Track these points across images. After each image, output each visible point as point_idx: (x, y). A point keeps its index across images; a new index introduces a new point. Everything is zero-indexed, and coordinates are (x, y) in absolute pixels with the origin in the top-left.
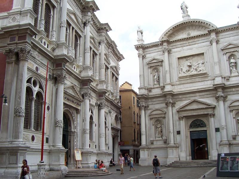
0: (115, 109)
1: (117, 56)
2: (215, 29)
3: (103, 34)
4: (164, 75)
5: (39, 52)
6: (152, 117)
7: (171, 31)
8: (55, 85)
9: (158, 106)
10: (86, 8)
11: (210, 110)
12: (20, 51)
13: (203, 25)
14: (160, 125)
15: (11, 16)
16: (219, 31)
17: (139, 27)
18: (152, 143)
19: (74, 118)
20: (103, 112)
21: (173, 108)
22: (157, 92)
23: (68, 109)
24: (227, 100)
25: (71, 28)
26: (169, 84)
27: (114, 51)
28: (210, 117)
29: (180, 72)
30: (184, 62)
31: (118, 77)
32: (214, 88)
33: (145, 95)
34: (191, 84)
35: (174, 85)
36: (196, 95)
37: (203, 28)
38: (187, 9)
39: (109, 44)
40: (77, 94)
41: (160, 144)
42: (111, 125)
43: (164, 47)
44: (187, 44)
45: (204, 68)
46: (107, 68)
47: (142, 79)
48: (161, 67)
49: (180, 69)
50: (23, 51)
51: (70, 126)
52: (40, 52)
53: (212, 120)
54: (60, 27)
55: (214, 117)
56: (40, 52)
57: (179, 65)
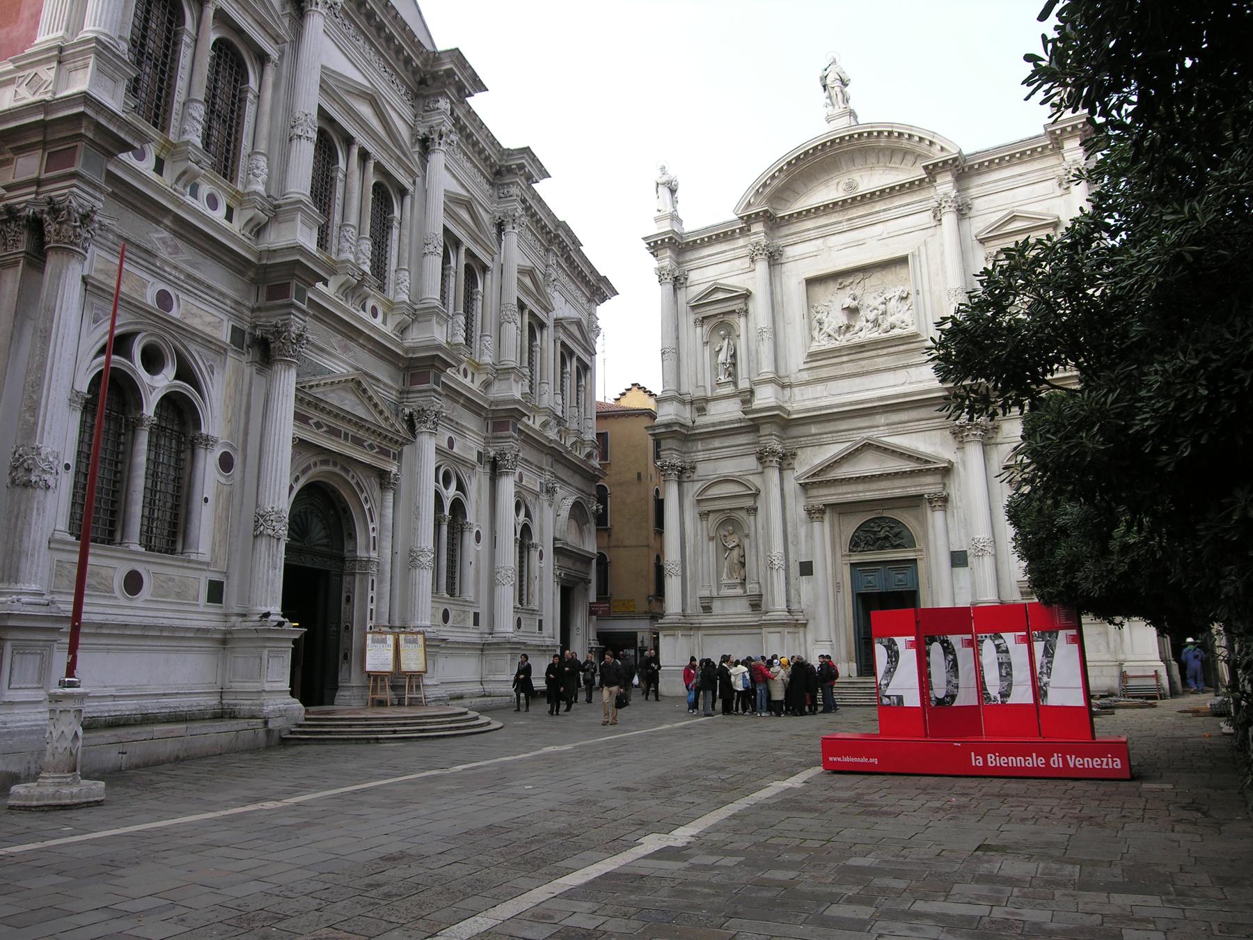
0: (577, 481)
1: (588, 284)
2: (955, 160)
3: (514, 190)
4: (753, 348)
5: (175, 233)
6: (707, 507)
7: (782, 176)
8: (259, 372)
9: (728, 468)
10: (430, 82)
11: (929, 479)
12: (48, 213)
13: (904, 143)
14: (737, 541)
15: (26, 73)
16: (971, 167)
17: (663, 168)
18: (707, 609)
19: (366, 507)
20: (507, 486)
21: (787, 473)
22: (726, 411)
23: (337, 470)
24: (999, 440)
25: (355, 150)
26: (770, 381)
27: (569, 259)
28: (929, 511)
29: (815, 334)
30: (830, 298)
31: (593, 361)
32: (946, 393)
33: (682, 425)
34: (857, 380)
35: (790, 386)
36: (875, 423)
37: (908, 157)
38: (847, 89)
39: (550, 232)
40: (381, 412)
41: (737, 610)
42: (555, 539)
43: (754, 239)
44: (845, 226)
45: (907, 317)
46: (536, 326)
47: (671, 363)
48: (743, 320)
49: (815, 323)
50: (60, 210)
51: (352, 536)
52: (181, 231)
53: (936, 519)
54: (291, 140)
56: (181, 231)
57: (810, 306)
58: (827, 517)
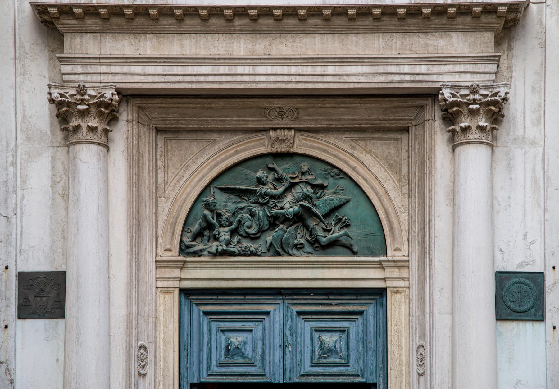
53: (464, 172)
55: (494, 138)
58: (120, 133)
